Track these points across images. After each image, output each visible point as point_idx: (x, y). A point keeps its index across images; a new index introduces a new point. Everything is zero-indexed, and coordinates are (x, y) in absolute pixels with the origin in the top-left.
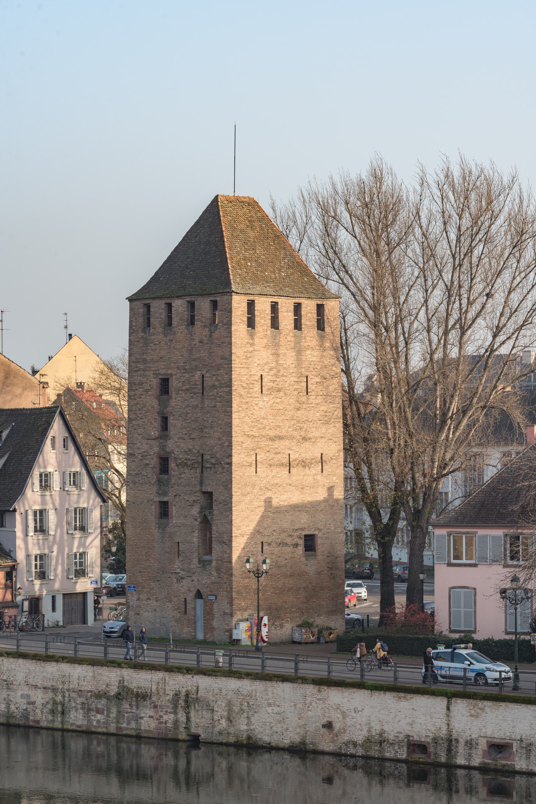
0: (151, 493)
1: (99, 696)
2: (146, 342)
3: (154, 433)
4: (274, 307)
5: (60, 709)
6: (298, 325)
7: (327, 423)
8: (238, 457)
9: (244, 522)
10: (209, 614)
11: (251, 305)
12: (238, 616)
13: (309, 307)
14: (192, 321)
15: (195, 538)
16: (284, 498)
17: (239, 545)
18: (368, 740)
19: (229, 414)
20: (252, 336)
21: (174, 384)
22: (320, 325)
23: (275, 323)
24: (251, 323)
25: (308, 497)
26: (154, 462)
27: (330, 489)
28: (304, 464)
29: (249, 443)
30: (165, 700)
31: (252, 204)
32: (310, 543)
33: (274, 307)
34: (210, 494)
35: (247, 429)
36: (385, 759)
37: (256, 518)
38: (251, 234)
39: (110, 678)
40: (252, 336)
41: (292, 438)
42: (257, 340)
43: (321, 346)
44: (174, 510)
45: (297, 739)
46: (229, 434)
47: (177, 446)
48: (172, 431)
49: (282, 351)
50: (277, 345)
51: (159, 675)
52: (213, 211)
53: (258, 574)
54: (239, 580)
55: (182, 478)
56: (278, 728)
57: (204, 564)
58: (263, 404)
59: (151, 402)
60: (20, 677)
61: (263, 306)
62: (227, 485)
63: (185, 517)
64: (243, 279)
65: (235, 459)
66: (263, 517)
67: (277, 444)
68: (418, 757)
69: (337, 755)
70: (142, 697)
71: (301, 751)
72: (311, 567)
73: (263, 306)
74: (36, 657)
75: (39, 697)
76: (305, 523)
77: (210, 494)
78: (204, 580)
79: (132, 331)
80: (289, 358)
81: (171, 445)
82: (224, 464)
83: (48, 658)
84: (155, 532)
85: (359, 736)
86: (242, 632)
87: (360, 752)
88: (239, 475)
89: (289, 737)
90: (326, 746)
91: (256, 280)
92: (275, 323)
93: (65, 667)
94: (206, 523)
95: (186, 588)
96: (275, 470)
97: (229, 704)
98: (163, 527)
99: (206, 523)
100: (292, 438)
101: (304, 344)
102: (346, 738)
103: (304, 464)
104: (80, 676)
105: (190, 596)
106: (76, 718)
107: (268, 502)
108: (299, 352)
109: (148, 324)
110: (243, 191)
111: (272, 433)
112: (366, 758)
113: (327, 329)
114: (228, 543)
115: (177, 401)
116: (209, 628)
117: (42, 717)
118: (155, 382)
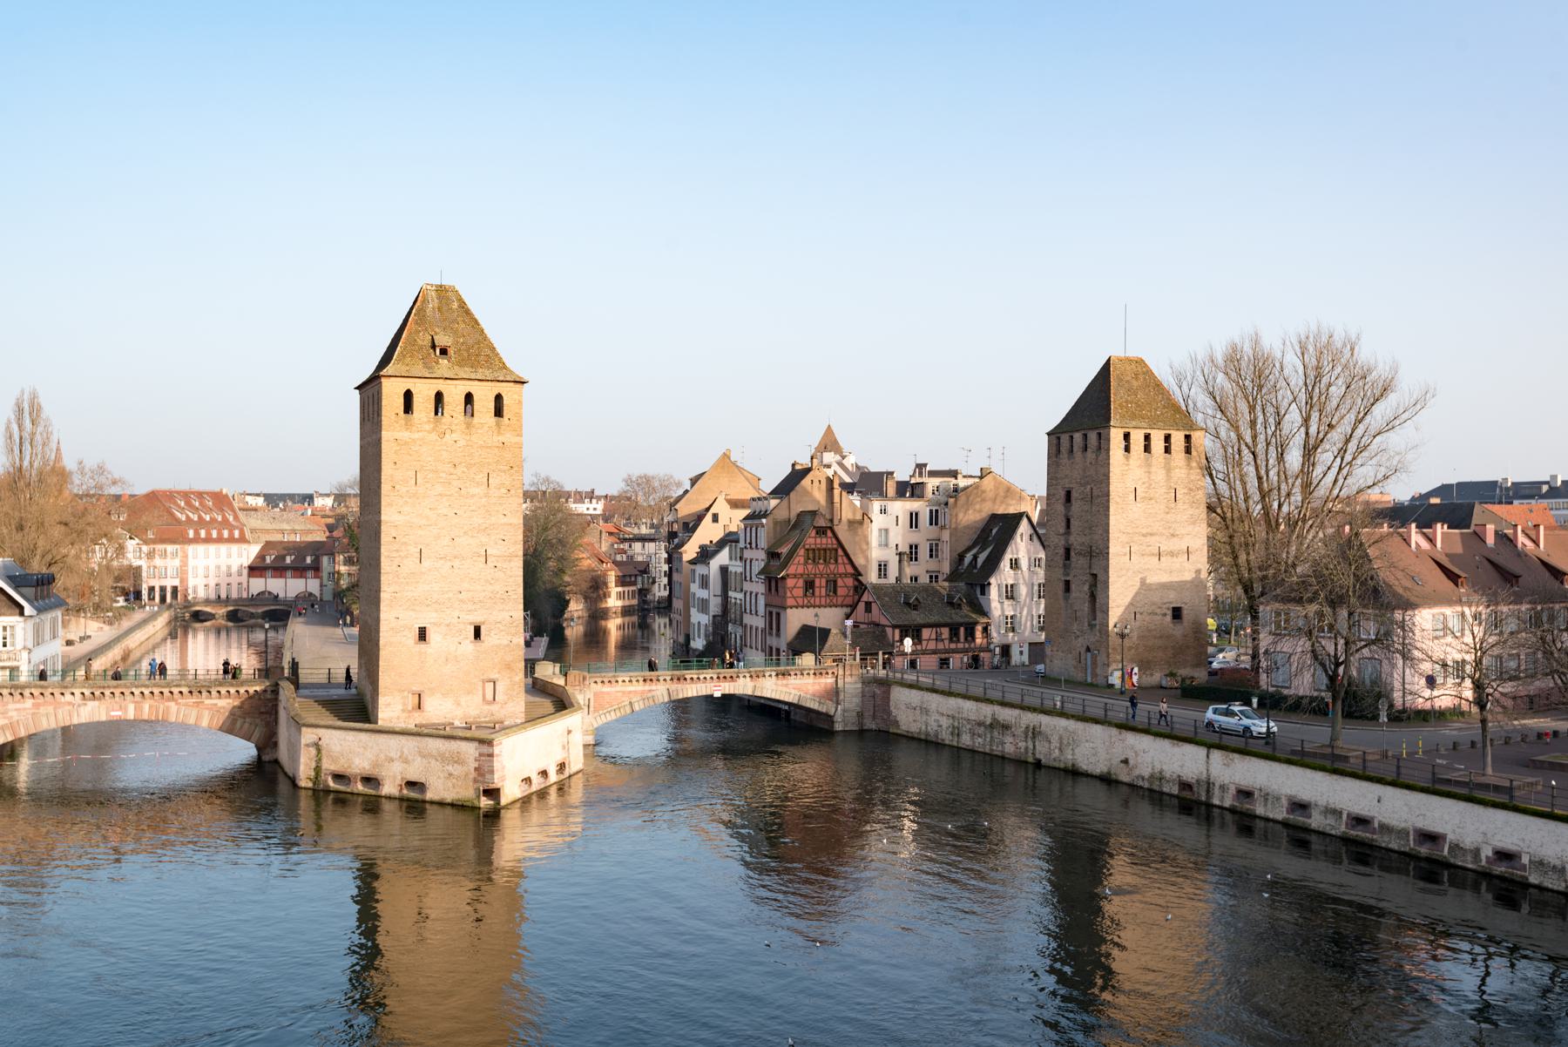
0: (1059, 574)
1: (980, 724)
2: (1058, 465)
3: (1062, 531)
4: (1147, 437)
5: (956, 732)
6: (1167, 450)
7: (1194, 523)
8: (1114, 549)
9: (1120, 597)
10: (1094, 663)
11: (1127, 436)
12: (1114, 666)
13: (1178, 438)
14: (1085, 449)
15: (1086, 607)
16: (1153, 579)
17: (1116, 613)
18: (1152, 776)
19: (1107, 516)
20: (1127, 458)
21: (1074, 495)
22: (1188, 451)
23: (1147, 449)
24: (1127, 449)
25: (1175, 578)
26: (1062, 551)
27: (1198, 572)
28: (1172, 554)
29: (1124, 538)
30: (1020, 731)
31: (1140, 362)
32: (1177, 613)
33: (1147, 437)
34: (1095, 576)
36: (1162, 793)
37: (1131, 595)
38: (1135, 384)
39: (987, 711)
40: (1127, 458)
41: (1162, 535)
45: (1105, 770)
46: (1107, 532)
47: (1076, 540)
48: (1073, 529)
49: (1153, 469)
50: (1149, 465)
51: (1016, 712)
52: (1107, 367)
53: (1122, 636)
54: (1114, 641)
55: (1078, 562)
56: (1092, 760)
57: (1092, 626)
58: (1137, 510)
59: (1060, 507)
60: (933, 707)
61: (1137, 438)
62: (1106, 569)
63: (1080, 591)
64: (1123, 417)
66: (1137, 594)
67: (1148, 539)
68: (1187, 794)
69: (1131, 786)
70: (1006, 727)
71: (1107, 780)
72: (1178, 631)
73: (1137, 438)
74: (943, 693)
75: (945, 722)
76: (1174, 599)
77: (1095, 576)
78: (1091, 639)
79: (1049, 458)
80: (1159, 474)
81: (1072, 539)
82: (1104, 554)
83: (950, 694)
84: (1062, 602)
85: (1146, 773)
86: (1115, 679)
87: (1146, 785)
88: (1114, 562)
89: (1099, 768)
90: (1125, 778)
91: (1133, 417)
92: (1147, 449)
93: (960, 701)
94: (1093, 597)
95: (1080, 644)
96: (1147, 559)
97: (1061, 738)
98: (1066, 599)
99: (1093, 597)
100: (1162, 535)
101: (1173, 464)
102: (1137, 772)
103: (1172, 554)
104: (968, 706)
105: (1083, 650)
106: (966, 740)
107: (1143, 581)
108: (1168, 470)
109: (1059, 451)
110: (1131, 354)
112: (1151, 790)
113: (1194, 453)
114: (1106, 612)
115: (1076, 506)
116: (1094, 675)
117: (946, 737)
118: (1063, 493)
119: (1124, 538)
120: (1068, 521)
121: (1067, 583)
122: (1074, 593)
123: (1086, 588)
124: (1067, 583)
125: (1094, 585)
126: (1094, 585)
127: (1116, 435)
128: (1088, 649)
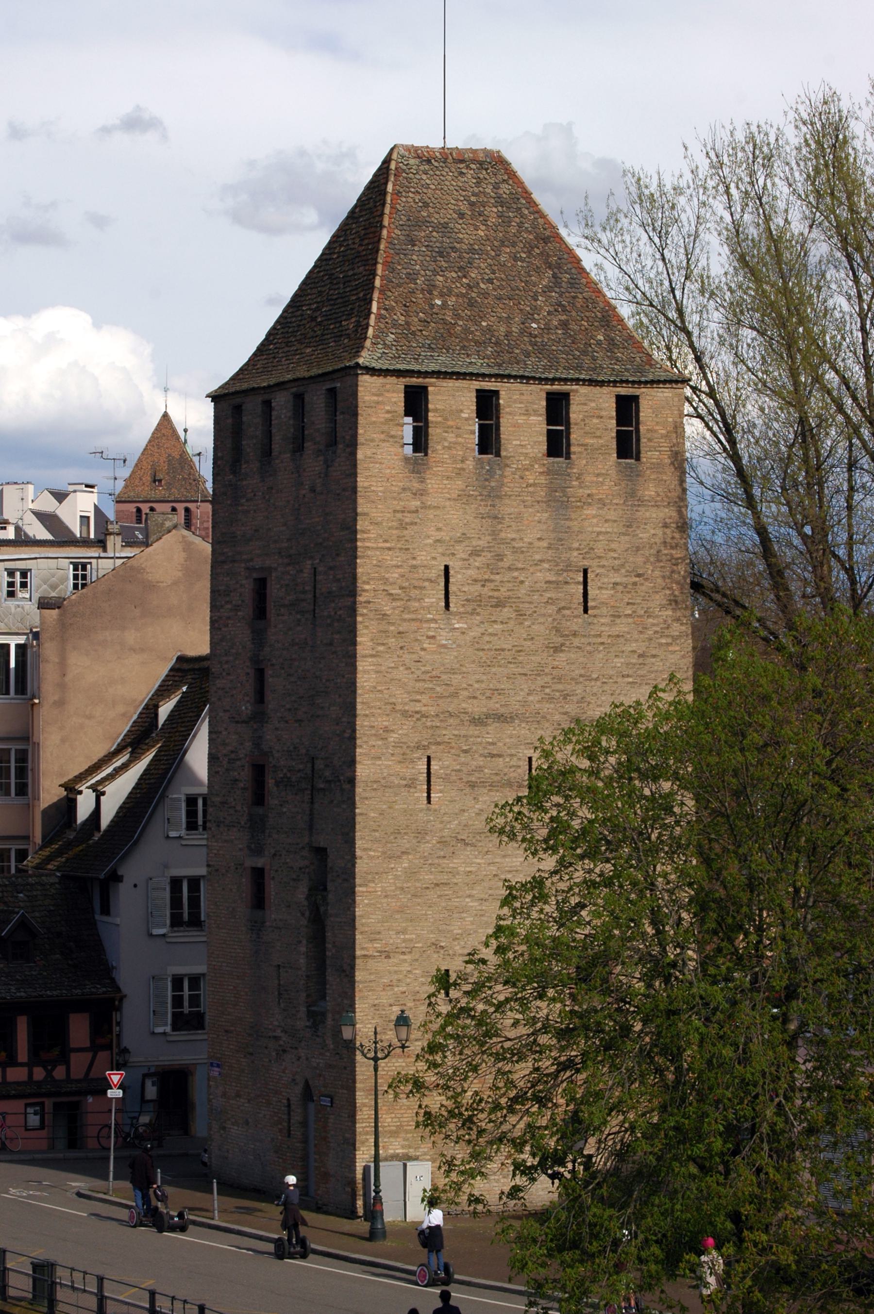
6: (557, 445)
22: (627, 446)
23: (489, 442)
35: (400, 696)
42: (432, 483)
43: (632, 496)
44: (272, 888)
49: (509, 508)
50: (493, 495)
58: (450, 638)
65: (364, 770)
77: (321, 852)
80: (531, 526)
101: (577, 491)
111: (476, 708)
119: (403, 730)
120: (260, 674)
121: (258, 875)
122: (274, 914)
123: (301, 893)
124: (258, 875)
125: (319, 888)
126: (319, 888)
127: (379, 402)
128: (308, 1094)
